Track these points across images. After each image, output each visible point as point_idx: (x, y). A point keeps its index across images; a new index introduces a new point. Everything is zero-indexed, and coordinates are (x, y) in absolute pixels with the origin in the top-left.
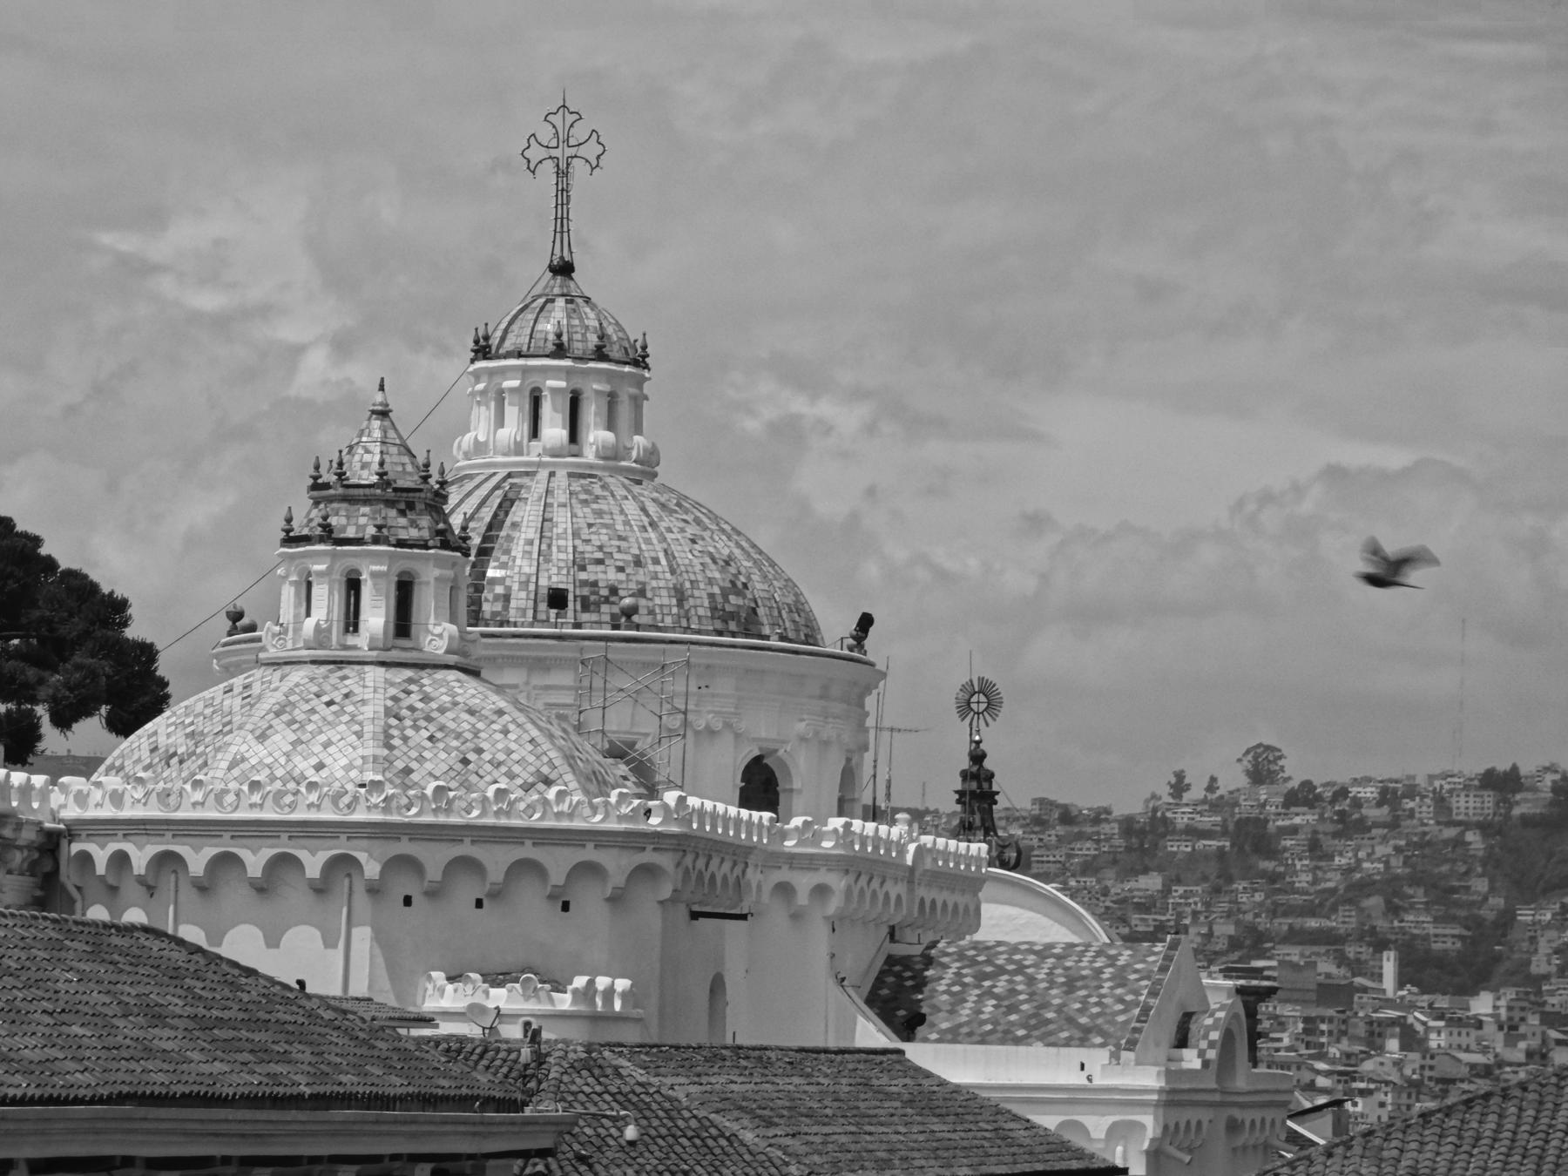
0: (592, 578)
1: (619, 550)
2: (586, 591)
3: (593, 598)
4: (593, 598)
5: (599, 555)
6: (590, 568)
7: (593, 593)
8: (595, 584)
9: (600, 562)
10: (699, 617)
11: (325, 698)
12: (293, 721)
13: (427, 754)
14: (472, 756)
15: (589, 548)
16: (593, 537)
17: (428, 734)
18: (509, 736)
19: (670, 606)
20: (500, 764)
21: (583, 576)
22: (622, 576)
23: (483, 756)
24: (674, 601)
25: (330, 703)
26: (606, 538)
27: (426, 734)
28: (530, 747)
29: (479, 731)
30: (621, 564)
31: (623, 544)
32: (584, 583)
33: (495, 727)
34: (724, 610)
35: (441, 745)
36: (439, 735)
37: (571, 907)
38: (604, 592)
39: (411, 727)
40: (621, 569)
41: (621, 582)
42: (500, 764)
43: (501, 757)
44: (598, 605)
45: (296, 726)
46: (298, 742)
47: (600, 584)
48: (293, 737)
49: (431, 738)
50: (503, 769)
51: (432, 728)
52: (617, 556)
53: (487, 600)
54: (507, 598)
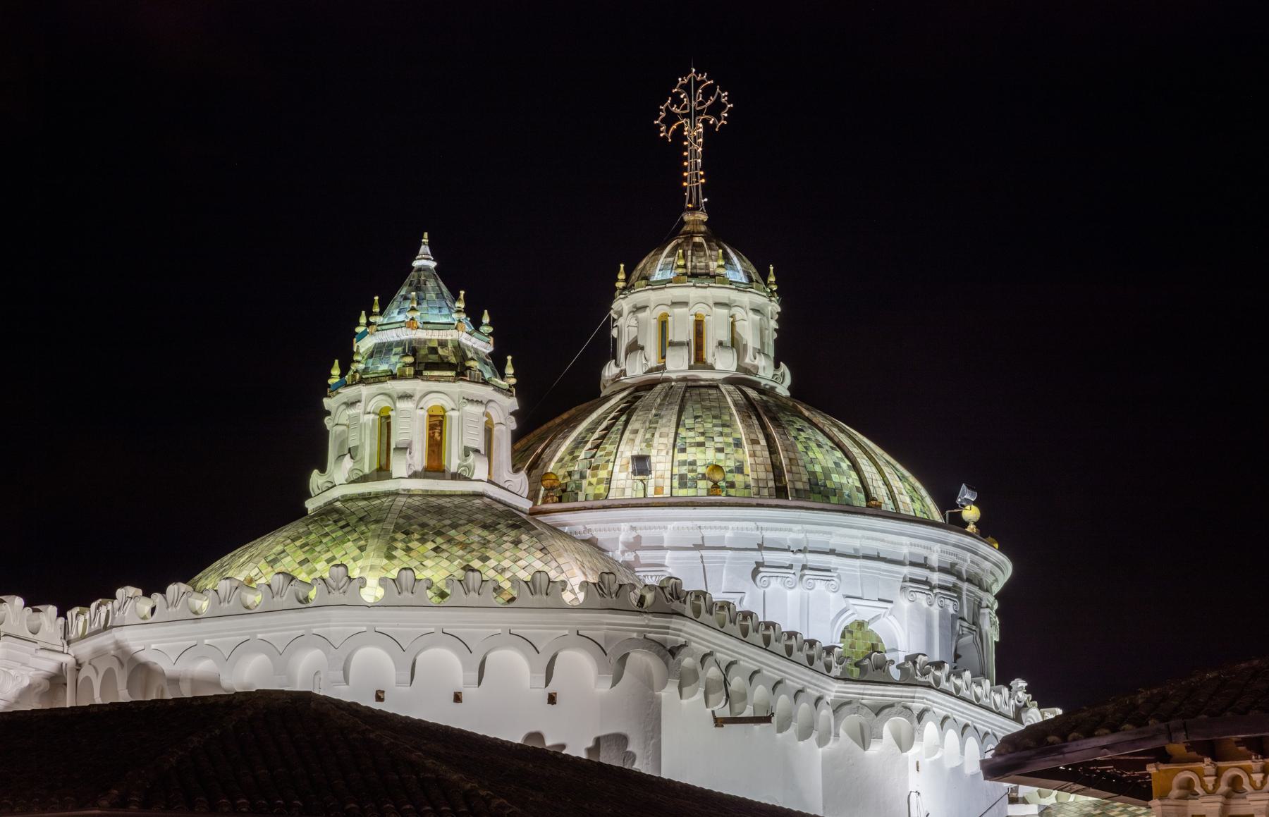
0: (690, 458)
1: (721, 434)
2: (684, 470)
3: (690, 475)
4: (690, 475)
5: (701, 439)
6: (689, 450)
7: (690, 471)
8: (693, 463)
9: (701, 444)
10: (797, 490)
11: (342, 523)
12: (306, 544)
13: (427, 563)
14: (476, 564)
15: (691, 434)
16: (697, 425)
17: (434, 546)
18: (520, 546)
19: (767, 481)
20: (504, 570)
21: (681, 457)
22: (721, 456)
23: (487, 563)
24: (771, 476)
25: (342, 528)
26: (710, 425)
27: (432, 545)
28: (539, 555)
29: (489, 542)
30: (719, 446)
31: (726, 430)
32: (683, 463)
33: (505, 538)
34: (826, 486)
35: (445, 555)
36: (444, 547)
37: (558, 699)
38: (701, 470)
39: (417, 540)
40: (720, 450)
41: (720, 460)
42: (504, 570)
43: (506, 563)
44: (695, 481)
45: (307, 548)
46: (305, 561)
47: (698, 463)
48: (303, 557)
49: (436, 549)
50: (508, 574)
51: (439, 540)
52: (717, 439)
53: (590, 484)
54: (609, 481)
